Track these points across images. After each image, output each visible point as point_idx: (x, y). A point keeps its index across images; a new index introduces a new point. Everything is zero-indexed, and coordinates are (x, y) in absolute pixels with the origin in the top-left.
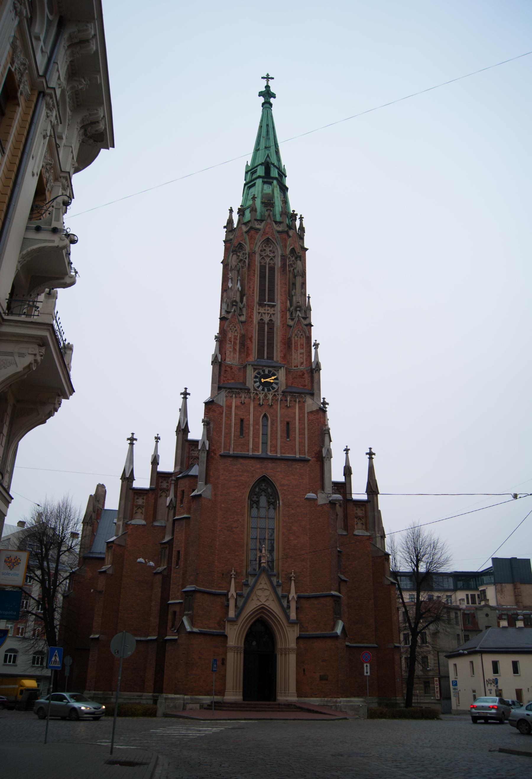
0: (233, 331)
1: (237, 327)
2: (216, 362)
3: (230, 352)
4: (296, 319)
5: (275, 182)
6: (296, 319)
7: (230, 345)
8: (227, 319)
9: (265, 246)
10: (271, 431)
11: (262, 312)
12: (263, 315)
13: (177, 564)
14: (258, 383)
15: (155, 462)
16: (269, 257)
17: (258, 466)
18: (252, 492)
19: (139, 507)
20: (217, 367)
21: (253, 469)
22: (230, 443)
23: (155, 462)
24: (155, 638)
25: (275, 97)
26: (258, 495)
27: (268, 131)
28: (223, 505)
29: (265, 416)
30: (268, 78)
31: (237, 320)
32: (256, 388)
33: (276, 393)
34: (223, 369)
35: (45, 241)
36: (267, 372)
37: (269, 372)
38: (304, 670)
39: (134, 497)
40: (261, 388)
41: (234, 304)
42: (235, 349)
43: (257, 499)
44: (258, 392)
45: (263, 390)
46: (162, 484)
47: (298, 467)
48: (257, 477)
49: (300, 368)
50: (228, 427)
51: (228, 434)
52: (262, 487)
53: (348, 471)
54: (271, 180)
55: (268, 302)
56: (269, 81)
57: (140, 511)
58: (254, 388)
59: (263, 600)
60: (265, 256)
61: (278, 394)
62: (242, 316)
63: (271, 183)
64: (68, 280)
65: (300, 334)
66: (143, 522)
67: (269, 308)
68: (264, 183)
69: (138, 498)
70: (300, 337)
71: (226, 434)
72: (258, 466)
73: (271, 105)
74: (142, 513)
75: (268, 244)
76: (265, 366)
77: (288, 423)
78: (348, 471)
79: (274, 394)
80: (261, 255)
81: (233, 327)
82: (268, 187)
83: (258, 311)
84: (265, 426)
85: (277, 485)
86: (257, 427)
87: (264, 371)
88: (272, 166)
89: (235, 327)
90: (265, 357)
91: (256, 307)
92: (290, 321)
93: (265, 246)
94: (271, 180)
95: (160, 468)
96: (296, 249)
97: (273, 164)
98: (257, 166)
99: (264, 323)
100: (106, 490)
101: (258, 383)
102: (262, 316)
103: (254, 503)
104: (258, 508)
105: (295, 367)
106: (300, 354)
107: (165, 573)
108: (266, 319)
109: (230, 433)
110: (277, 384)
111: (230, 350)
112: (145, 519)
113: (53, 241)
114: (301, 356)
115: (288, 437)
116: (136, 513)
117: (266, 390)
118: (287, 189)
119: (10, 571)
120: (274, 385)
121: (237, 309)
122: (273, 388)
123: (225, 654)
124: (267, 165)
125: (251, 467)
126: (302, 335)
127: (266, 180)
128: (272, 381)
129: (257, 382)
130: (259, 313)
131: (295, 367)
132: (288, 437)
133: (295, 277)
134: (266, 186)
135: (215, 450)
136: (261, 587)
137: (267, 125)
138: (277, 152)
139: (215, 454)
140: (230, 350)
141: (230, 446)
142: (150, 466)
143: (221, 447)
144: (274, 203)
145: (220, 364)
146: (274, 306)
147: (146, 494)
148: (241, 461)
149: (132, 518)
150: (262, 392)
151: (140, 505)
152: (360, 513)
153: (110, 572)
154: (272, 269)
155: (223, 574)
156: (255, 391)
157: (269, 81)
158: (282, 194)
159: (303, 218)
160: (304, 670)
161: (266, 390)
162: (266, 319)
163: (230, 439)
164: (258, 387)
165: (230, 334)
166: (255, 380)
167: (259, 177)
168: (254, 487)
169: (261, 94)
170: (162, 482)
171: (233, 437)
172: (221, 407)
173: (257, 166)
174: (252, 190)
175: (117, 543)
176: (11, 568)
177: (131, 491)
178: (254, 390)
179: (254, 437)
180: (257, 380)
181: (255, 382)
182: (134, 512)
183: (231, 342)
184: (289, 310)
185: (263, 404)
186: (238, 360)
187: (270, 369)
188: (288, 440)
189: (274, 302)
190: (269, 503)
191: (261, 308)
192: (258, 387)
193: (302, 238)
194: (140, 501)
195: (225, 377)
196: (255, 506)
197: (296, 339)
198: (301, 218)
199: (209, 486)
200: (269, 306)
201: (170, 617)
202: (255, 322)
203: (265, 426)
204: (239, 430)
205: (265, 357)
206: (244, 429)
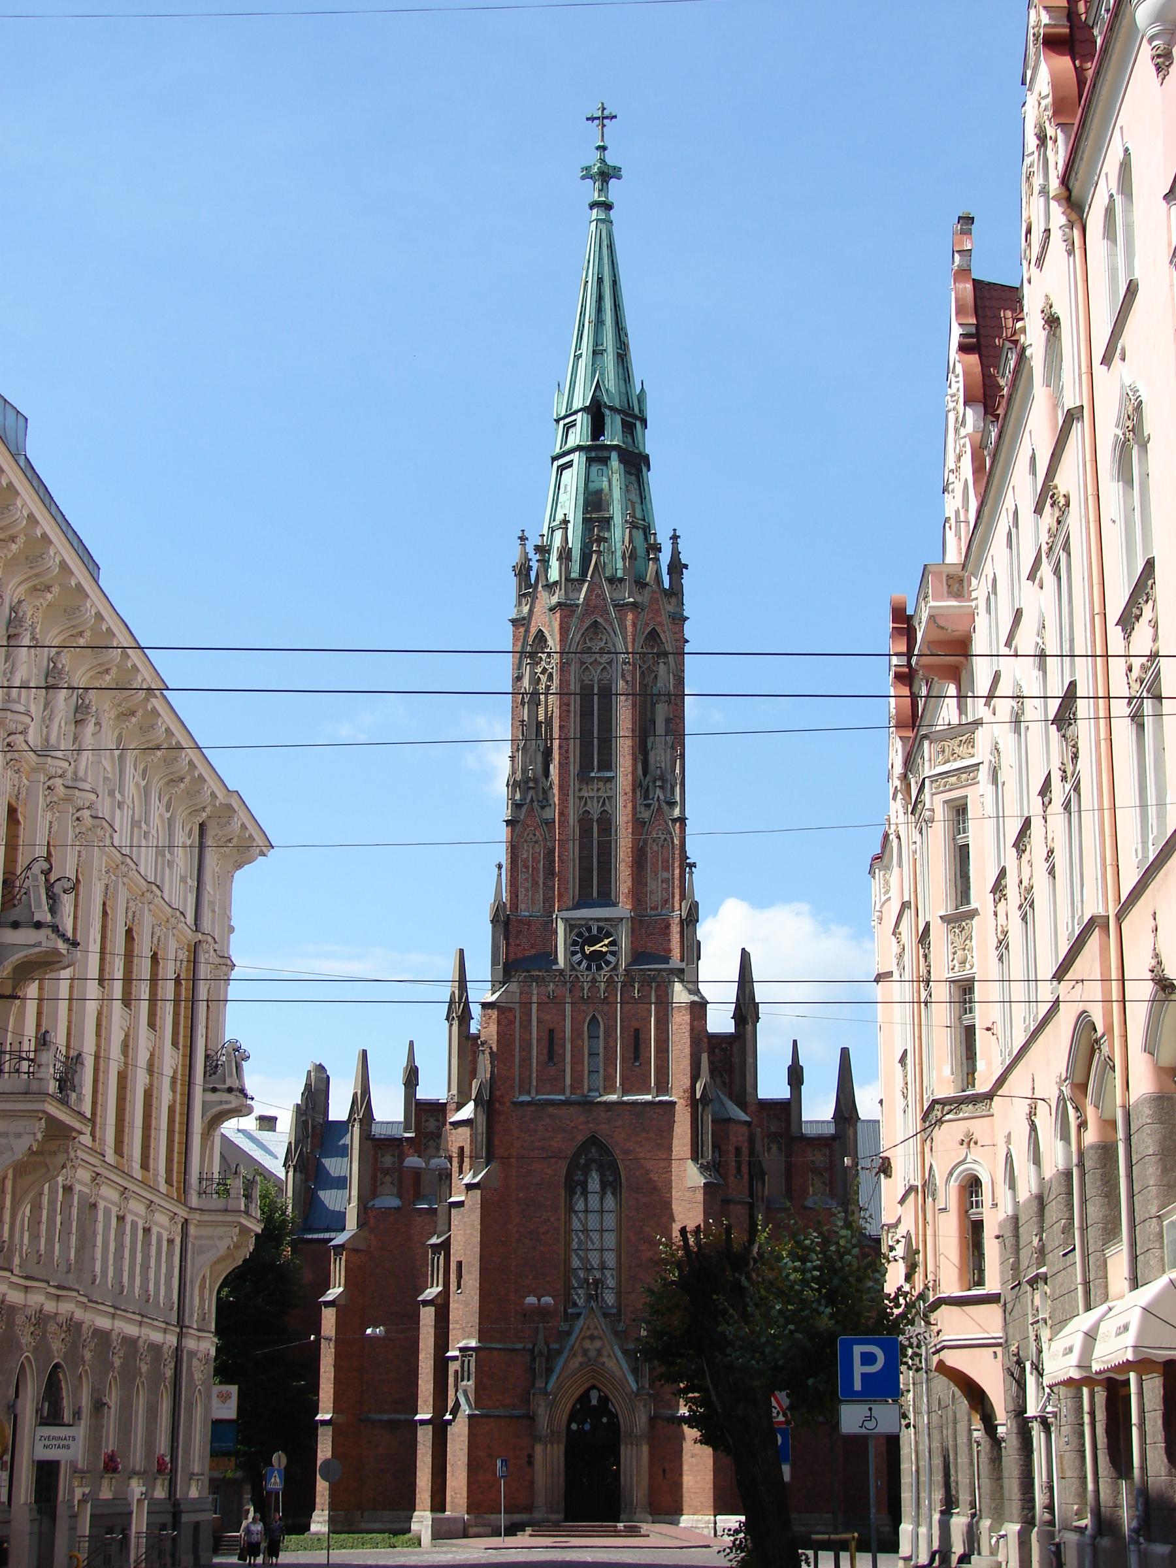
0: (531, 844)
1: (537, 833)
2: (498, 921)
3: (527, 890)
4: (655, 805)
5: (614, 455)
6: (655, 805)
7: (527, 875)
8: (518, 822)
9: (591, 639)
10: (605, 1048)
11: (586, 795)
12: (588, 800)
13: (459, 1287)
14: (579, 955)
15: (411, 1078)
16: (600, 664)
17: (582, 1119)
18: (572, 1167)
19: (387, 1172)
20: (501, 930)
21: (572, 1124)
22: (530, 1077)
23: (411, 1078)
24: (428, 1416)
25: (619, 178)
26: (586, 1171)
27: (600, 298)
28: (521, 1195)
29: (594, 1016)
30: (603, 118)
31: (538, 819)
32: (576, 966)
33: (615, 973)
34: (513, 930)
35: (221, 1102)
36: (595, 931)
37: (600, 929)
38: (664, 1471)
39: (377, 1153)
40: (584, 964)
41: (531, 785)
42: (535, 883)
43: (582, 1178)
44: (579, 974)
45: (589, 968)
46: (427, 1124)
47: (656, 1116)
48: (581, 1138)
49: (664, 912)
50: (526, 1046)
51: (526, 1061)
52: (590, 1156)
53: (796, 1075)
54: (605, 454)
55: (599, 770)
56: (604, 126)
57: (388, 1179)
58: (572, 965)
59: (592, 1354)
60: (591, 664)
61: (617, 975)
62: (547, 809)
63: (605, 461)
64: (245, 1111)
65: (663, 837)
66: (395, 1202)
67: (601, 784)
68: (590, 461)
69: (383, 1156)
70: (662, 846)
71: (522, 1060)
72: (582, 1119)
73: (608, 206)
74: (392, 1183)
75: (596, 633)
76: (591, 919)
77: (637, 1031)
78: (796, 1075)
79: (609, 974)
80: (583, 663)
81: (531, 836)
82: (600, 472)
83: (577, 794)
84: (593, 1037)
85: (617, 1153)
86: (579, 1042)
87: (589, 929)
88: (607, 412)
89: (535, 835)
90: (595, 894)
91: (574, 784)
92: (643, 808)
93: (591, 639)
94: (605, 454)
95: (422, 1094)
96: (659, 629)
97: (611, 408)
98: (576, 412)
99: (592, 820)
100: (328, 1077)
101: (579, 955)
102: (586, 803)
103: (574, 1186)
104: (585, 1193)
105: (652, 909)
106: (662, 882)
107: (439, 1301)
108: (595, 810)
109: (530, 1059)
110: (614, 953)
111: (526, 885)
112: (400, 1195)
113: (227, 1102)
114: (665, 886)
115: (636, 1058)
116: (382, 1183)
117: (594, 968)
118: (646, 459)
119: (222, 1405)
120: (609, 957)
121: (537, 794)
122: (608, 963)
123: (533, 1448)
124: (596, 412)
125: (568, 1122)
126: (665, 839)
127: (593, 454)
128: (604, 949)
129: (578, 952)
130: (581, 798)
131: (652, 909)
132: (636, 1058)
133: (653, 705)
134: (594, 469)
135: (502, 1096)
136: (588, 1334)
137: (600, 280)
138: (622, 357)
139: (503, 1104)
140: (526, 885)
141: (530, 1084)
142: (402, 1089)
143: (513, 1087)
144: (612, 518)
145: (507, 923)
146: (610, 779)
147: (399, 1146)
148: (551, 1110)
149: (374, 1194)
150: (587, 973)
151: (388, 1169)
152: (819, 1158)
153: (342, 1302)
154: (607, 694)
155: (525, 1315)
156: (573, 973)
157: (604, 126)
158: (633, 478)
159: (679, 537)
160: (664, 1471)
161: (594, 968)
162: (595, 810)
163: (531, 1070)
164: (580, 963)
165: (524, 852)
166: (572, 949)
167: (579, 448)
168: (577, 1155)
169: (587, 174)
170: (427, 1121)
171: (535, 1064)
172: (511, 1010)
173: (576, 412)
174: (567, 473)
175: (350, 1247)
176: (224, 1402)
177: (369, 1142)
178: (571, 970)
179: (573, 1064)
180: (578, 948)
181: (574, 953)
182: (379, 1183)
183: (527, 867)
184: (641, 785)
185: (588, 997)
186: (542, 904)
187: (601, 924)
188: (637, 1064)
189: (609, 769)
190: (604, 1185)
191: (584, 787)
192: (580, 963)
193: (676, 593)
194: (388, 1160)
195: (519, 945)
196: (579, 1190)
197: (655, 848)
198: (675, 538)
199: (494, 1165)
200: (600, 779)
201: (451, 1380)
202: (571, 822)
203: (593, 1037)
204: (545, 1051)
205: (595, 894)
206: (556, 1048)
